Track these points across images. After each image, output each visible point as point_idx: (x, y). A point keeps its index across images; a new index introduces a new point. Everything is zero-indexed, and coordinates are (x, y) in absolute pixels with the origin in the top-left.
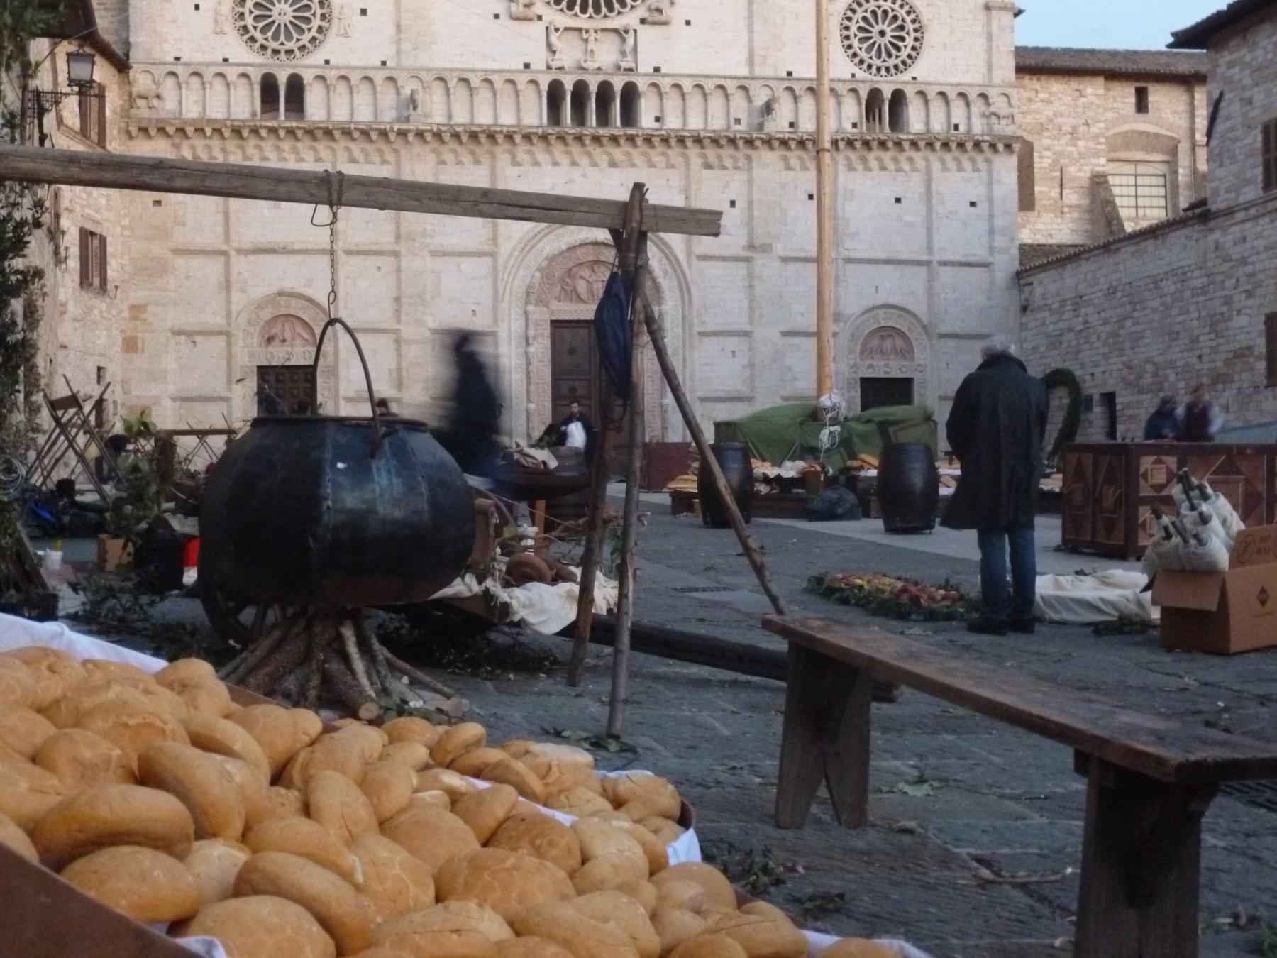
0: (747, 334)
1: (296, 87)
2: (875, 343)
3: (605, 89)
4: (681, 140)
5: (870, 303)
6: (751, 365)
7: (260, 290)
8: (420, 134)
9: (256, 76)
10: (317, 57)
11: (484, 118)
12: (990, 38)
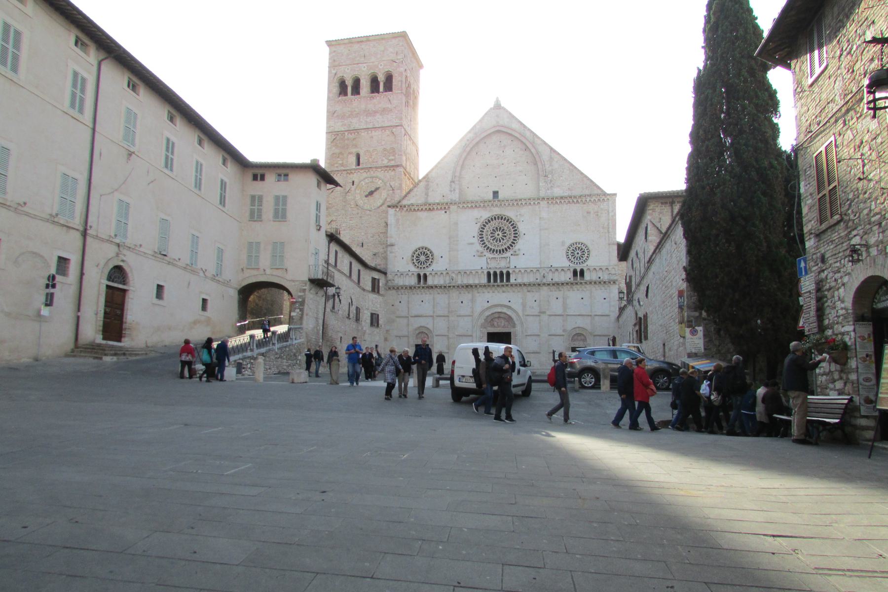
0: (539, 335)
1: (425, 276)
2: (576, 337)
3: (502, 273)
4: (520, 285)
5: (574, 327)
6: (540, 344)
7: (416, 326)
8: (454, 286)
9: (416, 274)
10: (430, 269)
11: (471, 282)
12: (610, 252)
